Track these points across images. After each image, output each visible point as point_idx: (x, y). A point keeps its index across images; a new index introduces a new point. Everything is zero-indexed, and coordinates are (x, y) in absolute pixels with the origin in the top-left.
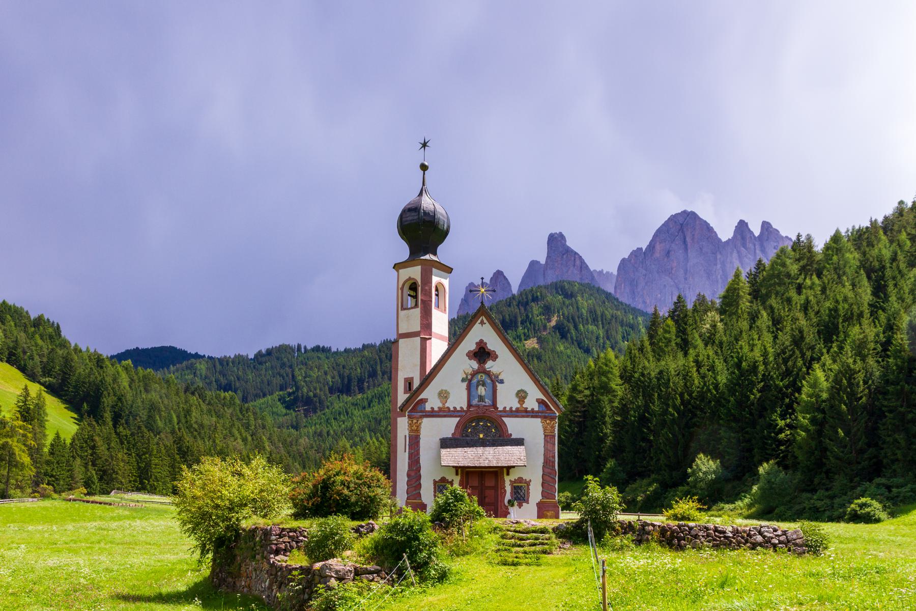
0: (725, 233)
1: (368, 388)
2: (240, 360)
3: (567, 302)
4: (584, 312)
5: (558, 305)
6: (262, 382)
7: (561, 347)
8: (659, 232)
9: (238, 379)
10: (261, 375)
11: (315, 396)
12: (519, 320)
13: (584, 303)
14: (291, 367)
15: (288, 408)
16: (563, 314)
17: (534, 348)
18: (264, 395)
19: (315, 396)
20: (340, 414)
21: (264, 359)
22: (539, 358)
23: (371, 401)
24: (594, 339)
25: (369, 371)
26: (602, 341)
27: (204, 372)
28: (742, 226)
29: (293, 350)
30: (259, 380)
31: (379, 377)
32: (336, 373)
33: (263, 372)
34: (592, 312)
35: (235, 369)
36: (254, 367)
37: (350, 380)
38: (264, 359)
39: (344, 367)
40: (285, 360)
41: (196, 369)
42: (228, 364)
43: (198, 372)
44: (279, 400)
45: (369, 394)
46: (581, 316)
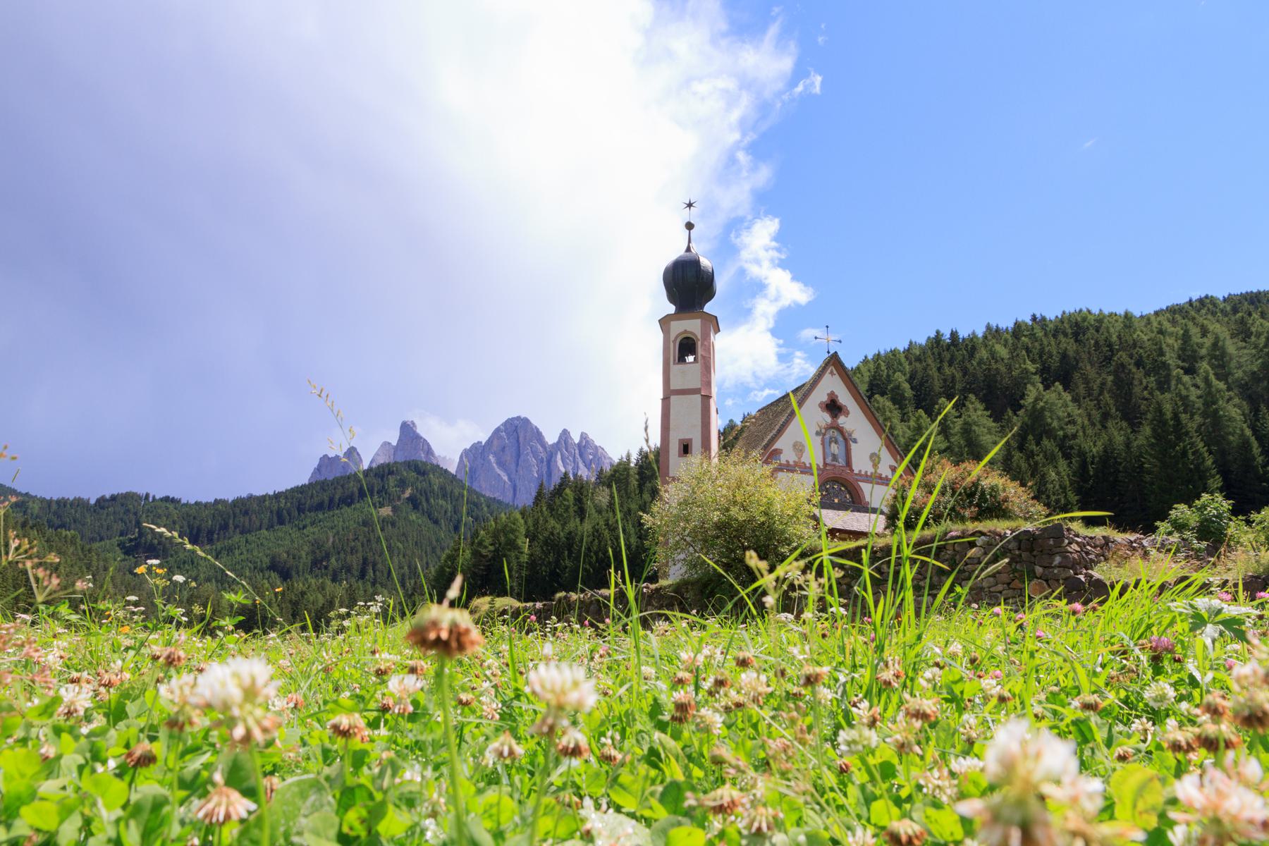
0: (551, 438)
1: (218, 540)
2: (80, 504)
3: (421, 478)
4: (436, 488)
5: (412, 480)
6: (102, 526)
7: (413, 517)
8: (498, 430)
9: (75, 522)
10: (101, 519)
11: (159, 543)
12: (376, 489)
13: (436, 482)
14: (135, 514)
15: (127, 553)
16: (417, 489)
17: (388, 515)
18: (101, 539)
19: (159, 543)
20: (184, 563)
21: (106, 504)
22: (393, 524)
23: (220, 552)
24: (443, 512)
25: (220, 524)
26: (449, 514)
27: (36, 511)
28: (565, 434)
29: (141, 498)
30: (98, 524)
31: (231, 530)
32: (185, 523)
33: (104, 516)
34: (442, 488)
35: (73, 511)
36: (95, 511)
37: (199, 530)
38: (106, 504)
39: (194, 518)
40: (131, 506)
41: (27, 508)
42: (65, 506)
43: (29, 511)
44: (119, 545)
45: (219, 545)
46: (432, 491)
